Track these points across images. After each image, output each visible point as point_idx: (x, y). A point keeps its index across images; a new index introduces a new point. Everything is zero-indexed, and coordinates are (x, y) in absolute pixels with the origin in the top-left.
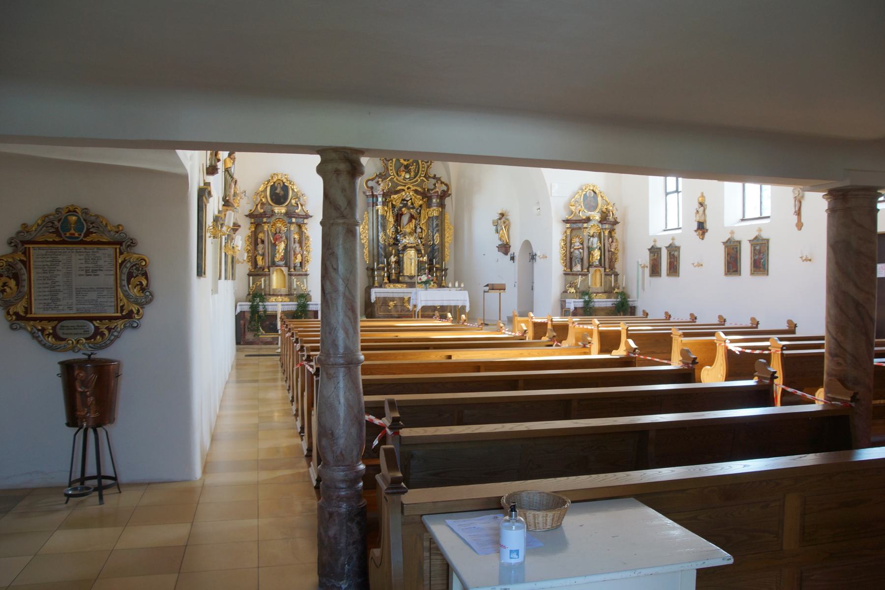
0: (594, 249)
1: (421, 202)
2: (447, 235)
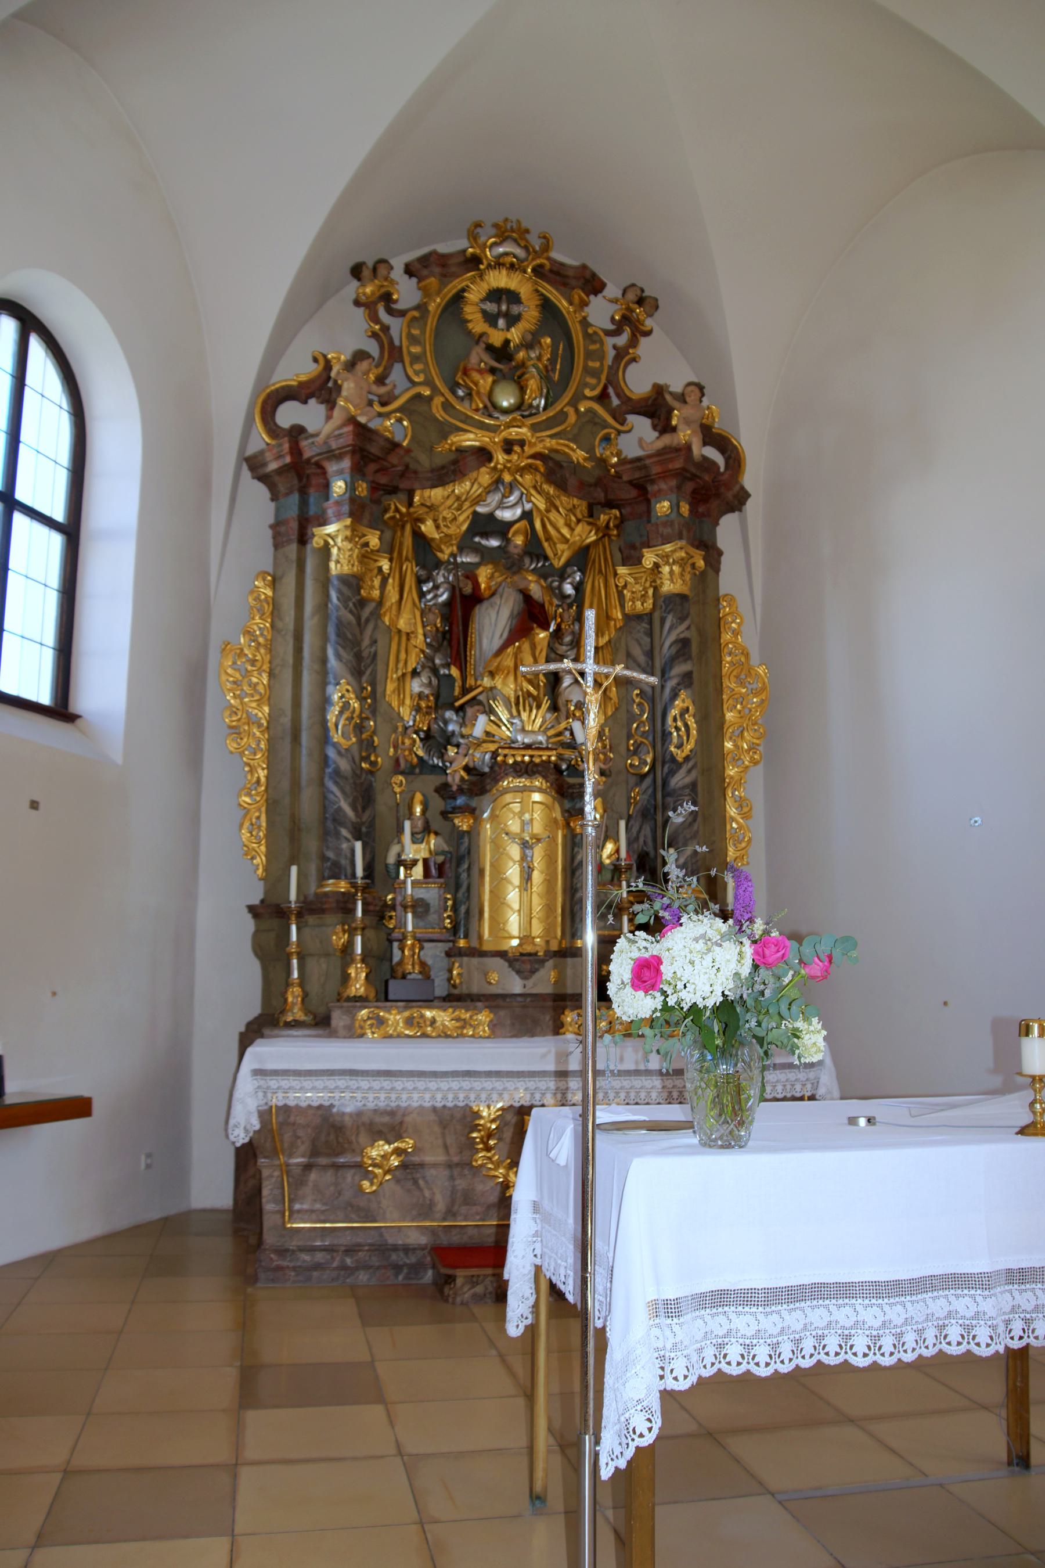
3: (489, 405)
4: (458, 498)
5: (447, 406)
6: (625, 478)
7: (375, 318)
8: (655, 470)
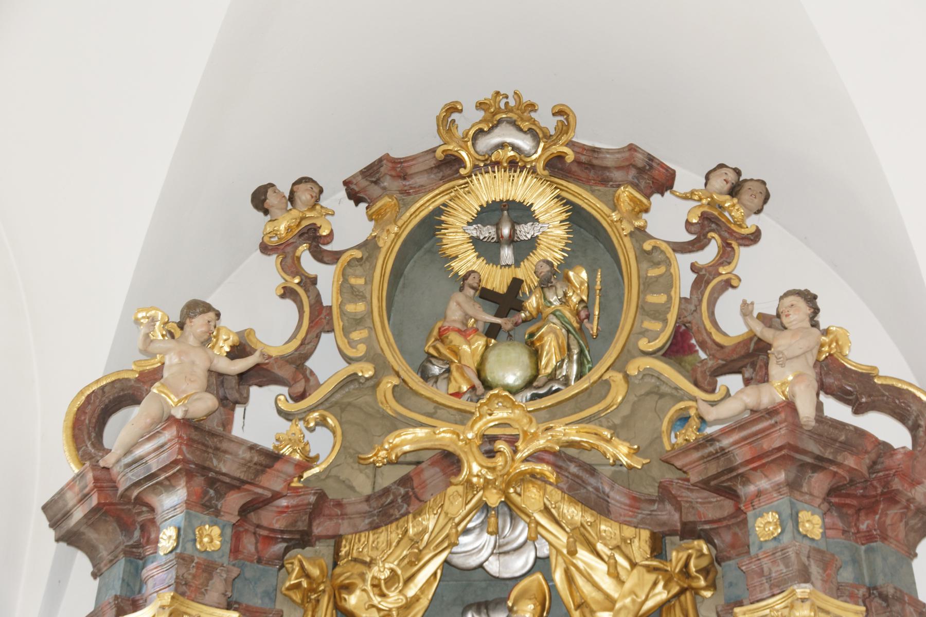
3: (477, 383)
4: (414, 542)
5: (402, 392)
6: (694, 478)
7: (291, 266)
8: (741, 455)
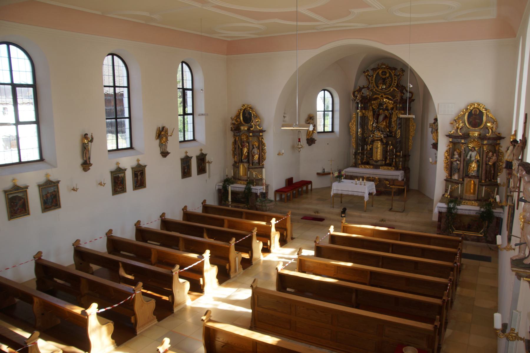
0: (472, 162)
1: (392, 106)
2: (411, 130)
5: (376, 90)
